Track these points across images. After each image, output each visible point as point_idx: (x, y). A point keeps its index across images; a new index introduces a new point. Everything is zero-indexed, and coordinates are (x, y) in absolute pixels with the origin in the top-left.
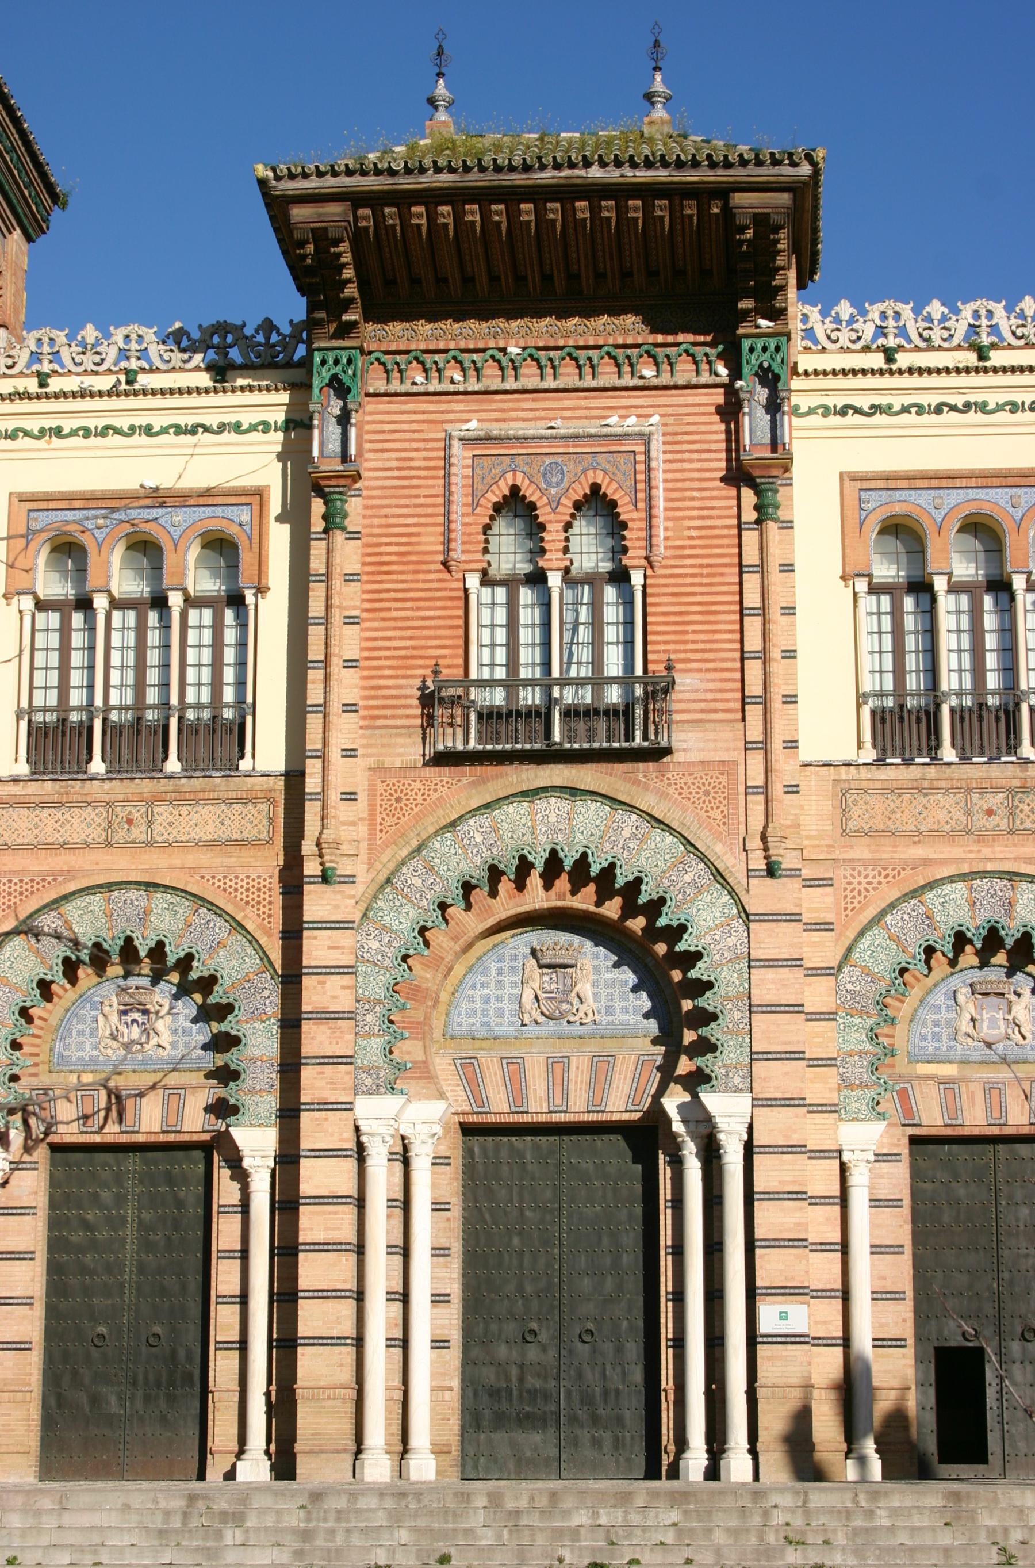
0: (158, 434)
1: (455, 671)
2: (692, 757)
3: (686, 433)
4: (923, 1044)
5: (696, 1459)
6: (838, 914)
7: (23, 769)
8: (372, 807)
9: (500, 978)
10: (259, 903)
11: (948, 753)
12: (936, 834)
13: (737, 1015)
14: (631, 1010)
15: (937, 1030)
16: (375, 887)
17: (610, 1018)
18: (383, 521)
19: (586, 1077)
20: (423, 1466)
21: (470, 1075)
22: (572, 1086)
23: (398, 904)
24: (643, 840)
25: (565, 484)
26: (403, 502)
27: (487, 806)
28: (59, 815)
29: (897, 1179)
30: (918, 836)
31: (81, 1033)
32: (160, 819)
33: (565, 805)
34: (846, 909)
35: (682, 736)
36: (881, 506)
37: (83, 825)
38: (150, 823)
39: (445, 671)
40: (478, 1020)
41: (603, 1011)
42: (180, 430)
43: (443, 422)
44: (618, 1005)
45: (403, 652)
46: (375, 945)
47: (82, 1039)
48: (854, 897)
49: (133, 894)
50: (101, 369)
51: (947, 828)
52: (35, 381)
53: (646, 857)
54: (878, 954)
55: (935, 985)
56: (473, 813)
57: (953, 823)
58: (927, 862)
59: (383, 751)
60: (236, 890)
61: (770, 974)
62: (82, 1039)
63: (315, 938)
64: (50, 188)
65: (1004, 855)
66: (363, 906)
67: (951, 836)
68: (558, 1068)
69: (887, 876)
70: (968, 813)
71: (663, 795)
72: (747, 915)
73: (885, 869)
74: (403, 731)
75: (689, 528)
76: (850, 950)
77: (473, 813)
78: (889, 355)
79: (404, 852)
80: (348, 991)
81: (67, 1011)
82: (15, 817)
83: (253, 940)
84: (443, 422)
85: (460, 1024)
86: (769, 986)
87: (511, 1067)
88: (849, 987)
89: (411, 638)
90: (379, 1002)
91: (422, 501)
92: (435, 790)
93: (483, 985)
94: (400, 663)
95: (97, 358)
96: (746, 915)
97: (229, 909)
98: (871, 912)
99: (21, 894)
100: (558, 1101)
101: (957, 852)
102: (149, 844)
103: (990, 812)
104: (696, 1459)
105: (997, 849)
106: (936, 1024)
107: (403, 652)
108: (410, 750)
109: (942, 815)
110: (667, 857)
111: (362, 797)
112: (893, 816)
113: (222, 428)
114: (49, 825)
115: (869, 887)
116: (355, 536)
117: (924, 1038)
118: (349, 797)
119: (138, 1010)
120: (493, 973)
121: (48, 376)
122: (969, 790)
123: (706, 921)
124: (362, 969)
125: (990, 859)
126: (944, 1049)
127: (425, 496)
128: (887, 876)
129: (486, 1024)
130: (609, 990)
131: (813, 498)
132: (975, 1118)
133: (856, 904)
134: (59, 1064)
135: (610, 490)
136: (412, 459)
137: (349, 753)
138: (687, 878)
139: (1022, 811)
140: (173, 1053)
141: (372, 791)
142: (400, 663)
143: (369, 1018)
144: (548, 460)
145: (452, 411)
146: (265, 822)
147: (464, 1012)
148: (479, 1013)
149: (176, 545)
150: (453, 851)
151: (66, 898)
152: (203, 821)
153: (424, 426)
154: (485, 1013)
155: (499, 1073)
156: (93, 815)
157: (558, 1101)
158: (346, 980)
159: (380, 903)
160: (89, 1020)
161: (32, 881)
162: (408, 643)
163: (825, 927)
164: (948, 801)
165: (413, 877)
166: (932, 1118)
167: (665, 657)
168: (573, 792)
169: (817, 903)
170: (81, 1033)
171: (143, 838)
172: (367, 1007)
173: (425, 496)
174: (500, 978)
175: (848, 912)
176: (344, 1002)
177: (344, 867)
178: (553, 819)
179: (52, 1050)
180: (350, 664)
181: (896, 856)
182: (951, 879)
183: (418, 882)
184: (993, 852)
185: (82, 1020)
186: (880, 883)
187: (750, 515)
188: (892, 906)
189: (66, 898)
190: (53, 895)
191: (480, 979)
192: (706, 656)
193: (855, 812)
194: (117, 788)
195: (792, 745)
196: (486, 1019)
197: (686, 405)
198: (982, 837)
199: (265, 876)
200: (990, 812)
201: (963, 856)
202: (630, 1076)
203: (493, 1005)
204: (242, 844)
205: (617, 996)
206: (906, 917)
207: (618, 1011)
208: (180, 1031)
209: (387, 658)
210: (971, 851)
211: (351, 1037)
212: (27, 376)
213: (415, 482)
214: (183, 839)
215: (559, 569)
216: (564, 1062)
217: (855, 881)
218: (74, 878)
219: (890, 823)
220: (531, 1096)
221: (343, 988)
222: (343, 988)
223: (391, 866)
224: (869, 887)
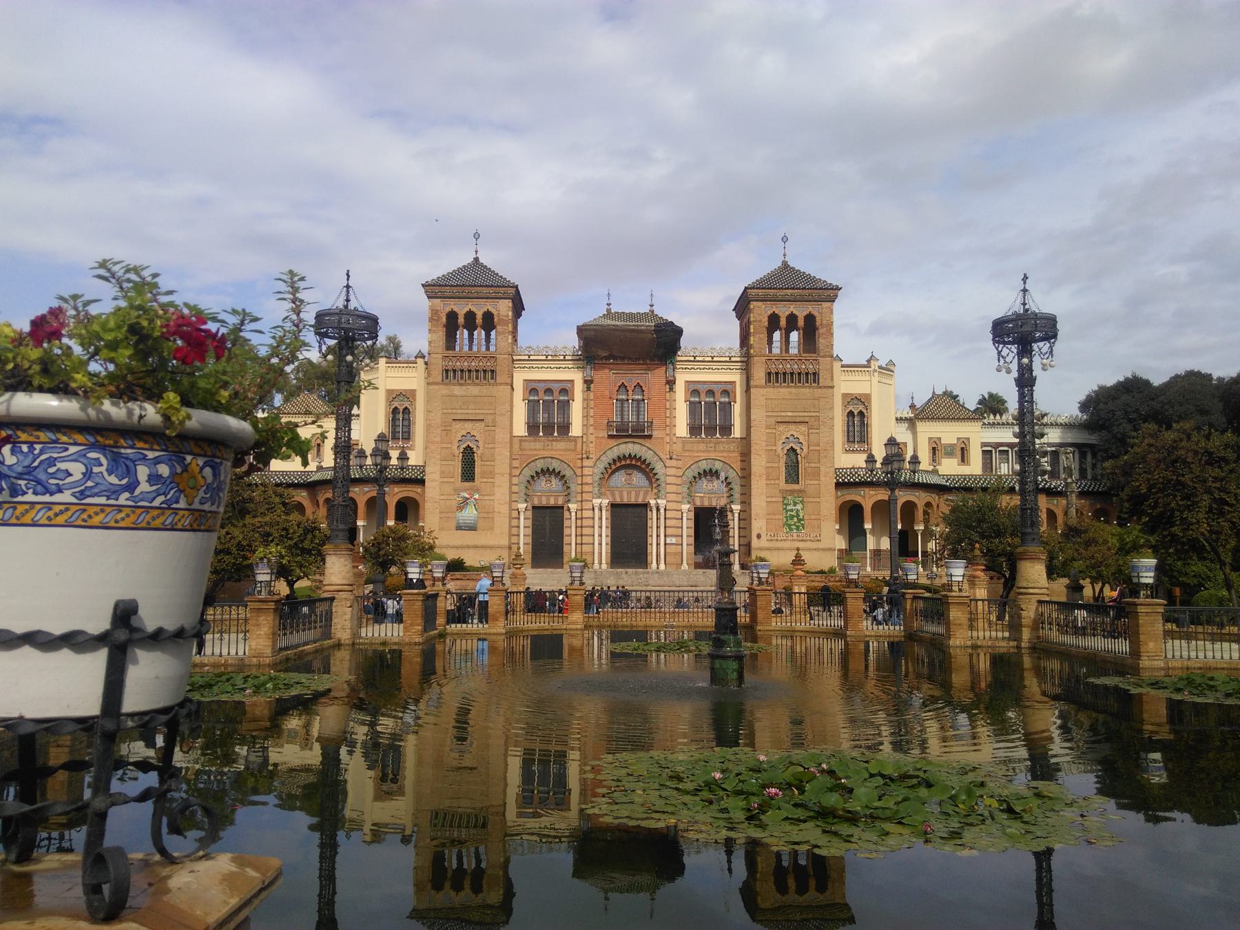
5: (654, 565)
20: (604, 566)
29: (692, 515)
36: (692, 387)
37: (538, 445)
54: (690, 474)
65: (713, 455)
86: (669, 480)
104: (654, 565)
108: (604, 434)
123: (659, 468)
131: (680, 388)
132: (706, 504)
134: (534, 491)
152: (561, 445)
165: (603, 458)
166: (698, 503)
169: (679, 464)
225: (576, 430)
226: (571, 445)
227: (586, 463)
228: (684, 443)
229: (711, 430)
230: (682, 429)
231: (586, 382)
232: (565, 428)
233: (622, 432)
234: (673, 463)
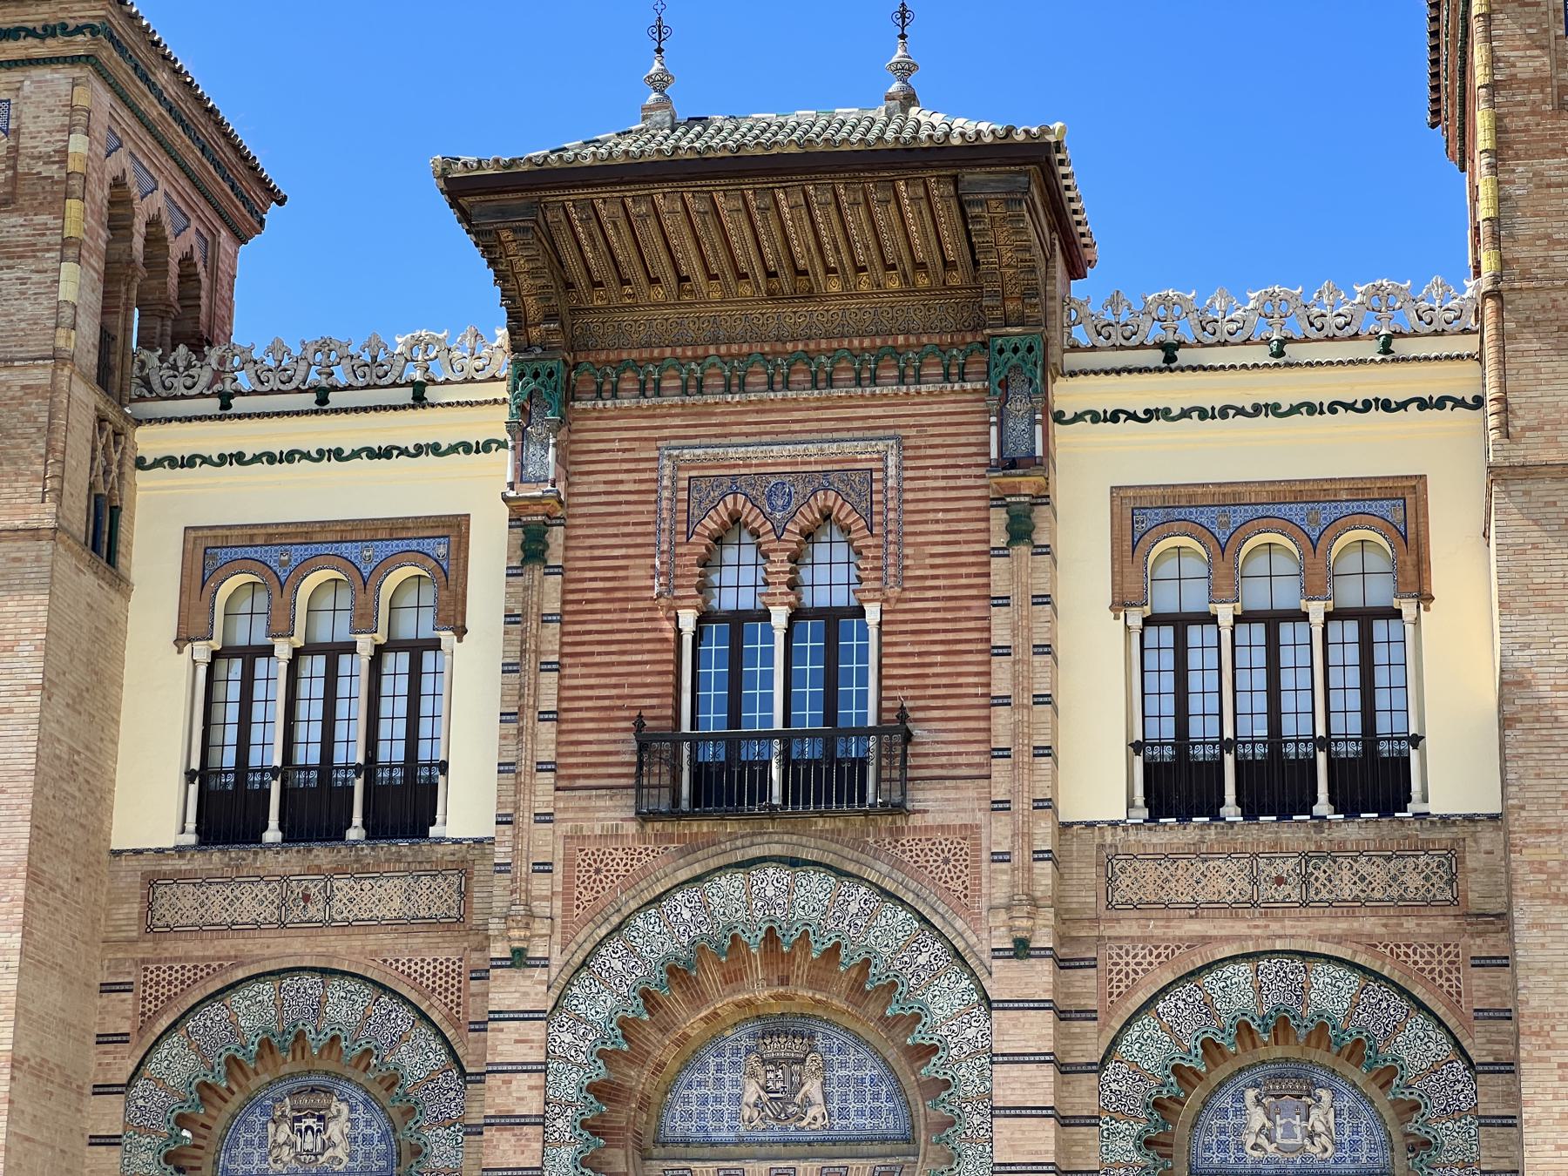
0: (347, 459)
1: (664, 723)
2: (929, 820)
3: (931, 447)
4: (1207, 1155)
6: (1102, 1000)
7: (191, 839)
8: (567, 879)
9: (720, 1075)
10: (446, 990)
11: (1231, 811)
12: (1218, 907)
13: (977, 1119)
14: (867, 1113)
15: (1223, 1138)
16: (568, 971)
17: (844, 1122)
18: (587, 553)
23: (595, 990)
24: (872, 916)
25: (793, 507)
26: (610, 531)
27: (697, 879)
28: (228, 892)
30: (1196, 910)
31: (249, 1143)
32: (340, 895)
33: (785, 875)
34: (1111, 994)
35: (919, 795)
37: (252, 903)
38: (328, 900)
39: (648, 723)
40: (692, 1125)
41: (836, 1114)
42: (373, 454)
43: (656, 440)
44: (853, 1106)
45: (607, 703)
46: (568, 1038)
47: (250, 1150)
48: (1120, 980)
49: (308, 980)
50: (192, 392)
51: (1229, 899)
52: (216, 402)
53: (886, 934)
54: (1150, 1048)
55: (1221, 1085)
56: (679, 886)
57: (1235, 893)
58: (1205, 940)
59: (582, 815)
60: (422, 975)
61: (1015, 1070)
62: (250, 1150)
63: (501, 1030)
64: (264, 183)
65: (1298, 932)
66: (554, 993)
67: (1233, 909)
69: (1159, 956)
70: (1254, 882)
71: (897, 864)
72: (989, 1002)
73: (1157, 948)
74: (604, 792)
75: (933, 556)
76: (1114, 1043)
77: (679, 886)
78: (1170, 351)
79: (603, 931)
80: (535, 1092)
81: (234, 1117)
82: (179, 894)
83: (439, 1033)
84: (656, 440)
85: (673, 1129)
86: (1014, 1086)
88: (1114, 1086)
89: (615, 686)
90: (570, 1104)
91: (630, 529)
92: (639, 860)
93: (699, 1084)
94: (602, 714)
95: (189, 382)
96: (988, 1003)
97: (413, 996)
98: (1141, 997)
99: (183, 982)
101: (1240, 928)
102: (328, 923)
103: (1280, 881)
105: (1287, 922)
106: (1222, 1131)
107: (607, 703)
109: (1223, 884)
110: (899, 935)
111: (558, 868)
112: (1166, 887)
113: (420, 450)
114: (217, 905)
115: (1139, 969)
116: (550, 571)
117: (1208, 1148)
118: (544, 868)
119: (313, 1116)
120: (712, 1068)
121: (231, 396)
122: (1255, 856)
124: (553, 1065)
125: (1280, 937)
126: (1232, 1161)
127: (635, 524)
128: (1159, 956)
129: (704, 1128)
133: (1123, 989)
135: (844, 513)
136: (621, 482)
137: (544, 818)
138: (922, 960)
139: (1317, 879)
140: (351, 1164)
141: (568, 862)
142: (602, 714)
143: (559, 1123)
144: (773, 481)
145: (666, 427)
146: (455, 896)
149: (282, 586)
150: (657, 929)
151: (232, 987)
153: (636, 445)
156: (266, 891)
158: (536, 1080)
159: (576, 990)
160: (258, 1127)
161: (195, 967)
162: (614, 692)
163: (1088, 1015)
164: (1230, 868)
165: (612, 960)
167: (897, 704)
168: (794, 863)
170: (249, 1143)
171: (320, 916)
172: (557, 1110)
173: (635, 524)
174: (720, 1075)
175: (1114, 998)
176: (533, 1106)
177: (538, 951)
178: (770, 892)
179: (216, 1163)
180: (544, 716)
181: (1170, 933)
182: (1234, 959)
183: (618, 965)
184: (1283, 927)
185: (250, 1128)
186: (1151, 964)
187: (999, 539)
188: (1164, 990)
189: (232, 987)
190: (219, 985)
191: (698, 1076)
192: (949, 702)
193: (1124, 881)
194: (292, 860)
195: (1045, 805)
196: (703, 1123)
197: (931, 415)
198: (1268, 909)
199: (454, 958)
200: (1280, 881)
201: (1247, 932)
204: (431, 923)
205: (851, 1096)
206: (1181, 1004)
208: (360, 1139)
209: (588, 709)
210: (1256, 927)
211: (539, 1146)
212: (208, 396)
213: (624, 508)
214: (365, 916)
215: (782, 604)
217: (1122, 962)
218: (242, 964)
219: (1162, 894)
221: (531, 1088)
222: (531, 1088)
223: (588, 946)
224: (1139, 969)
225: (465, 810)
226: (434, 897)
227: (509, 991)
228: (1109, 862)
229: (1275, 785)
230: (1099, 780)
231: (518, 512)
232: (406, 804)
233: (704, 782)
234: (1038, 978)
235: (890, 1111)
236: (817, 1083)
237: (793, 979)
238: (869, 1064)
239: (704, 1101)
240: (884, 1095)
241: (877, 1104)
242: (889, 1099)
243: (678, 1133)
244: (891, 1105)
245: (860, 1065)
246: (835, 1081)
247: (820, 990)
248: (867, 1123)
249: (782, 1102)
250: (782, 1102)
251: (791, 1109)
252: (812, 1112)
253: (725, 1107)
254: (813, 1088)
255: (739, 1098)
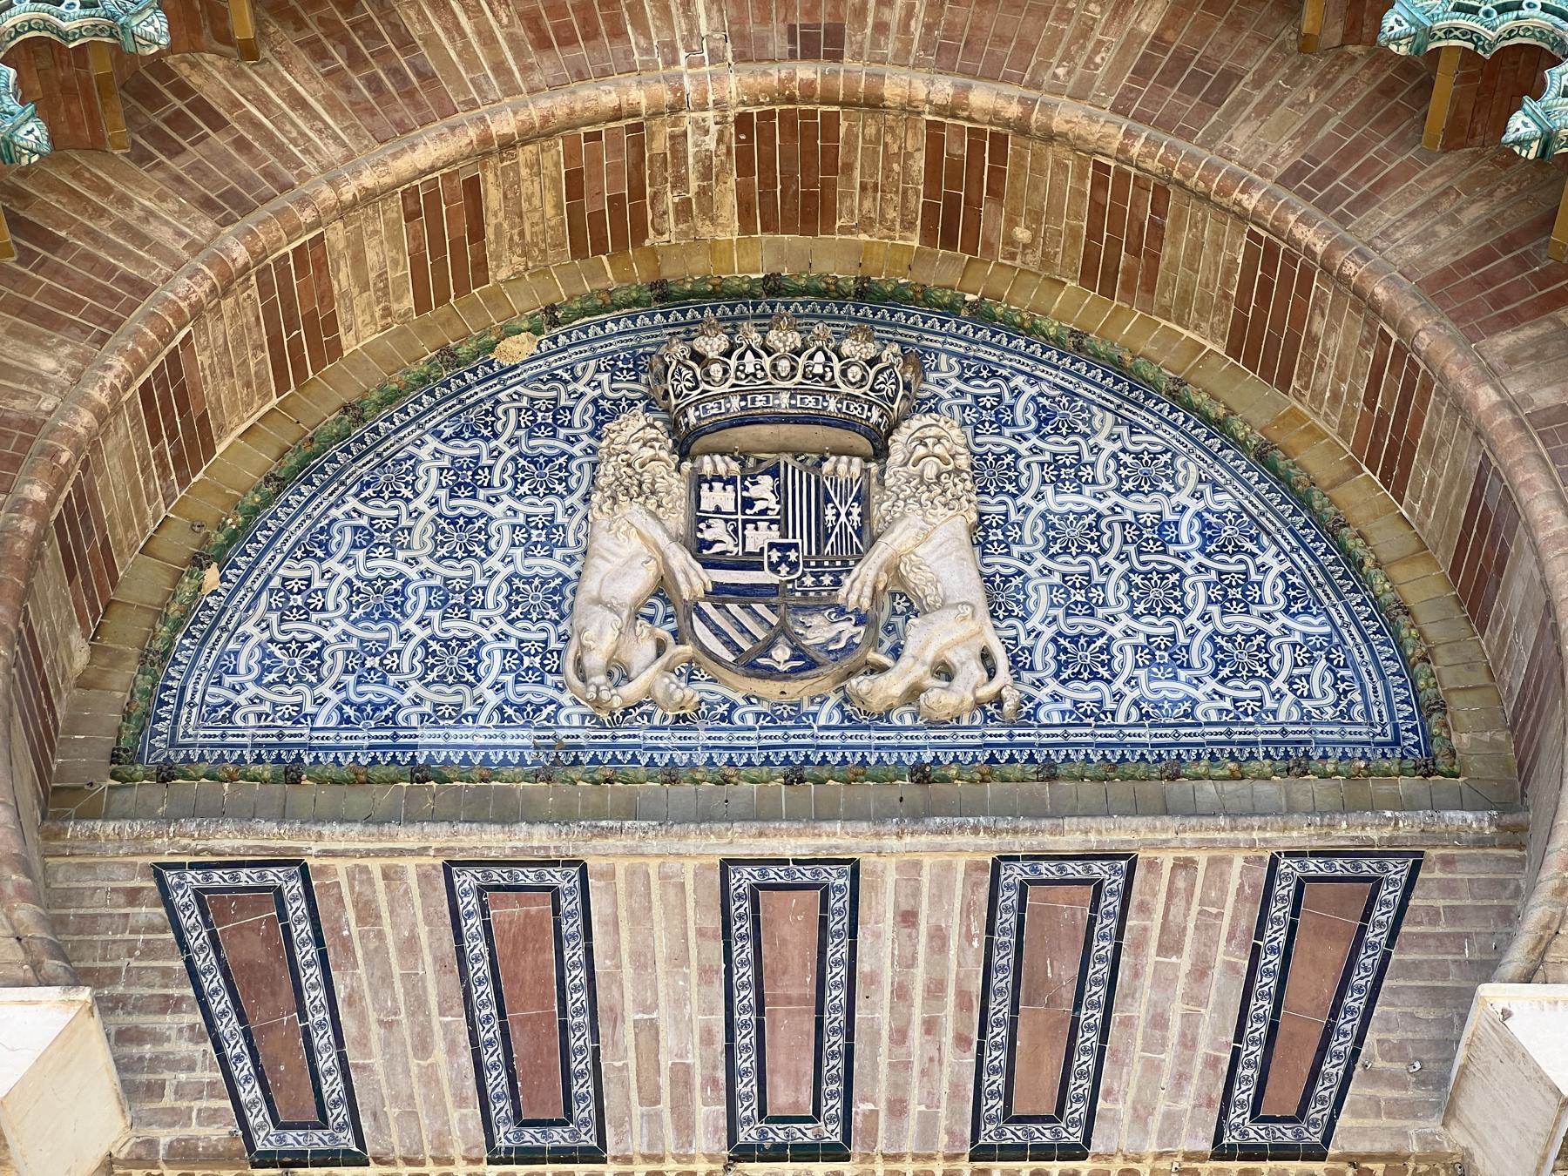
14: (1200, 652)
17: (1087, 693)
19: (962, 963)
21: (252, 949)
22: (875, 1013)
41: (1044, 658)
44: (1124, 629)
68: (791, 923)
85: (224, 714)
87: (506, 912)
93: (366, 538)
100: (789, 1094)
120: (430, 483)
130: (1074, 566)
147: (248, 658)
148: (334, 664)
154: (369, 662)
155: (433, 941)
157: (789, 1094)
196: (372, 692)
202: (1229, 957)
203: (418, 623)
205: (1114, 590)
207: (1125, 661)
216: (837, 896)
220: (621, 1058)
235: (1308, 651)
236: (952, 526)
237: (858, 36)
238: (1190, 470)
239: (387, 601)
240: (1271, 590)
241: (1238, 622)
242: (1297, 599)
243: (246, 727)
244: (1316, 626)
245: (1145, 474)
246: (1032, 531)
247: (991, 75)
248: (1209, 699)
249: (782, 588)
250: (782, 588)
251: (819, 631)
252: (928, 639)
253: (490, 627)
254: (926, 540)
255: (558, 597)
